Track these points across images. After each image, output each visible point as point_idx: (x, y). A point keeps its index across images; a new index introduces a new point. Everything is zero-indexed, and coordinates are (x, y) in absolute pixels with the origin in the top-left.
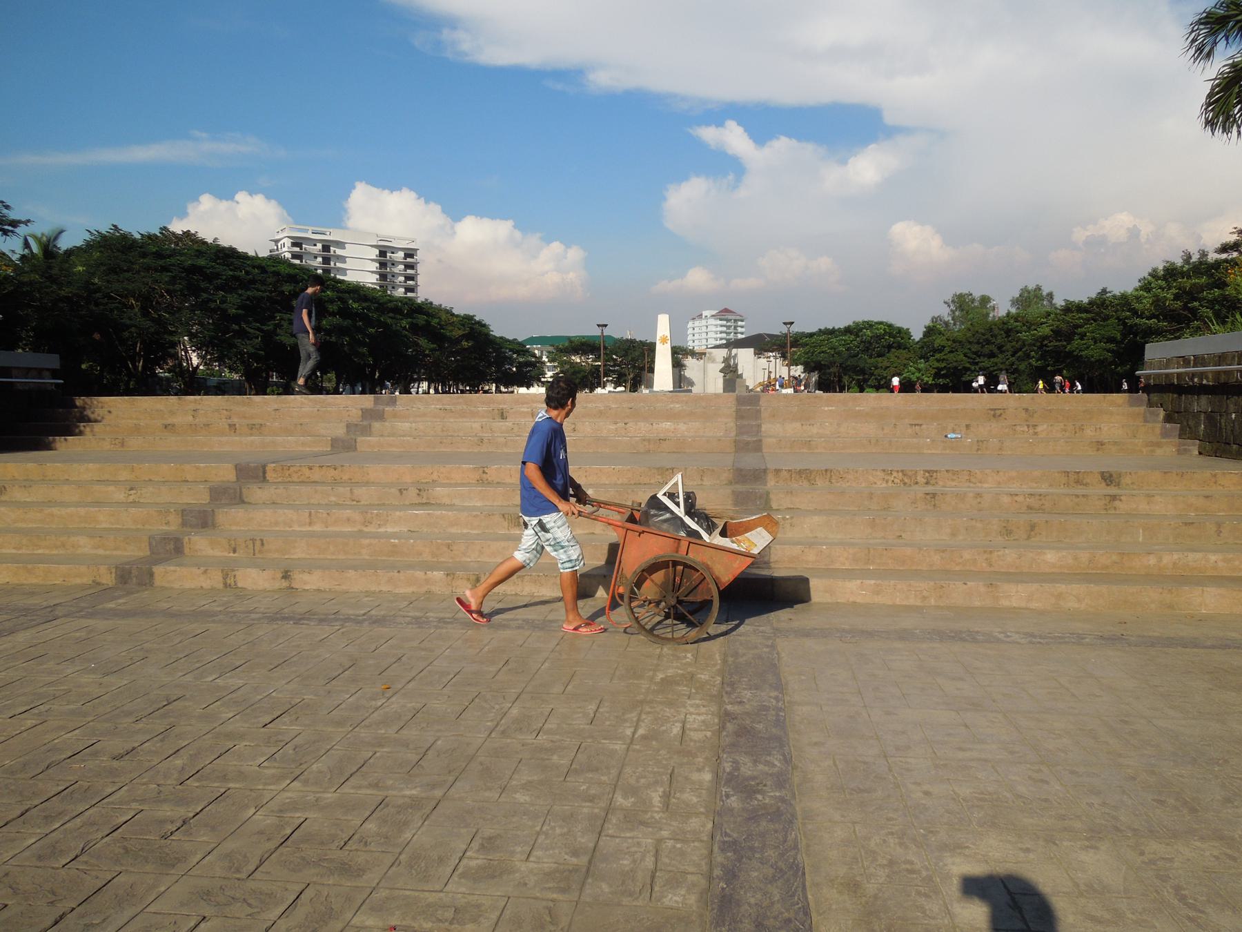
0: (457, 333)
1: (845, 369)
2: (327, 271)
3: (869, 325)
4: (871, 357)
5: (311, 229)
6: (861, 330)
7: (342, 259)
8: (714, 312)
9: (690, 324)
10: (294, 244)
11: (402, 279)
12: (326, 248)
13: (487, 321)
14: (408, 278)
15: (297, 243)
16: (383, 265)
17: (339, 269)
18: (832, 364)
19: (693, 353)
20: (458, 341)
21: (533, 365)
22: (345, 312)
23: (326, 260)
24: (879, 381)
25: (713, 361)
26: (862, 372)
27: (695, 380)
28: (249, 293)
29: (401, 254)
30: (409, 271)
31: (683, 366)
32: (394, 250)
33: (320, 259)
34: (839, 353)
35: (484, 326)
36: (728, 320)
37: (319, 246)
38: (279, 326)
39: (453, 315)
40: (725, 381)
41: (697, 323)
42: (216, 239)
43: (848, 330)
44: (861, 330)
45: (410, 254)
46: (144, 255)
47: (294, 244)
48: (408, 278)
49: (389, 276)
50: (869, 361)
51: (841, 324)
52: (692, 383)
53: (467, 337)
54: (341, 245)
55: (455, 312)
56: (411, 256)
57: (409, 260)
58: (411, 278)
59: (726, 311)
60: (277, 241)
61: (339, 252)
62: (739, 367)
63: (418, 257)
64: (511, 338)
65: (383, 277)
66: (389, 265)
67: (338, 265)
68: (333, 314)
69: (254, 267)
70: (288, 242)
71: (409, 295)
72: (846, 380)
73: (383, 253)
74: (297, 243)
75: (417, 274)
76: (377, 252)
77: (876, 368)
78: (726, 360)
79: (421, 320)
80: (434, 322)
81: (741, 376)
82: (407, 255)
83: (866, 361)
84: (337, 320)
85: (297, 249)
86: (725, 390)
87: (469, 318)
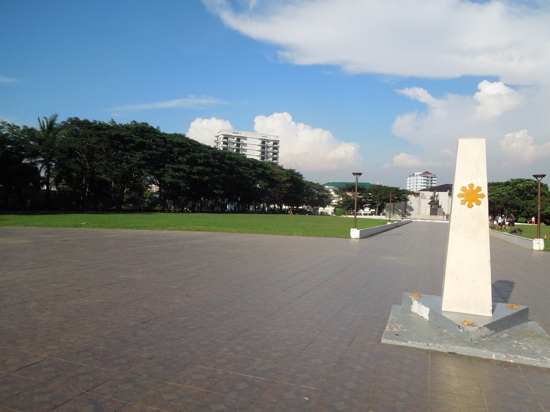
0: (284, 179)
1: (506, 205)
2: (238, 150)
3: (522, 181)
4: (523, 199)
6: (516, 183)
7: (245, 145)
8: (421, 173)
9: (408, 179)
10: (224, 138)
11: (271, 154)
12: (238, 140)
13: (301, 173)
14: (274, 154)
15: (226, 137)
16: (263, 148)
17: (244, 150)
18: (499, 203)
20: (284, 183)
21: (327, 197)
22: (207, 164)
23: (238, 145)
24: (528, 214)
25: (425, 198)
26: (518, 208)
27: (414, 208)
28: (150, 152)
29: (272, 143)
30: (275, 151)
31: (408, 200)
32: (269, 141)
33: (235, 145)
34: (502, 196)
35: (301, 176)
36: (427, 177)
37: (236, 139)
38: (165, 171)
39: (283, 170)
40: (431, 209)
41: (412, 178)
42: (158, 127)
43: (507, 184)
44: (516, 183)
45: (276, 143)
46: (90, 128)
47: (224, 138)
48: (274, 154)
49: (266, 153)
50: (522, 202)
51: (503, 180)
52: (412, 209)
53: (288, 181)
54: (245, 138)
55: (285, 167)
56: (276, 144)
58: (276, 154)
59: (427, 172)
60: (217, 137)
61: (244, 141)
63: (280, 144)
64: (316, 183)
65: (263, 153)
66: (266, 147)
67: (243, 147)
68: (201, 165)
69: (160, 138)
70: (222, 137)
71: (274, 161)
72: (506, 211)
73: (263, 142)
74: (226, 137)
75: (278, 152)
76: (261, 141)
77: (527, 206)
78: (432, 198)
79: (260, 170)
80: (268, 172)
81: (440, 207)
82: (274, 143)
83: (519, 201)
84: (201, 168)
85: (226, 140)
87: (291, 172)
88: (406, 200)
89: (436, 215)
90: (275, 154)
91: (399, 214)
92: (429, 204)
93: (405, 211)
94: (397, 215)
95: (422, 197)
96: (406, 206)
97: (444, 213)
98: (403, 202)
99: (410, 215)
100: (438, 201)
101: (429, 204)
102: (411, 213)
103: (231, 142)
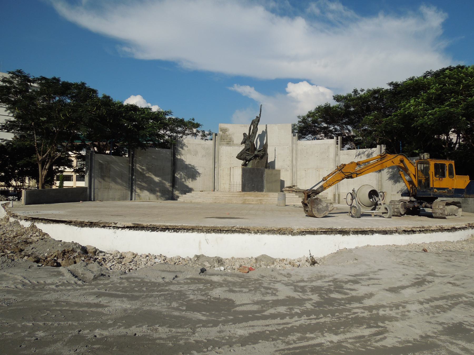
19: (190, 126)
25: (229, 142)
27: (200, 171)
40: (243, 170)
62: (270, 151)
78: (248, 139)
86: (244, 189)
88: (173, 146)
89: (260, 189)
91: (152, 191)
92: (239, 157)
93: (174, 181)
94: (146, 194)
95: (222, 139)
96: (176, 164)
97: (282, 182)
98: (167, 152)
99: (188, 190)
100: (264, 148)
101: (239, 157)
102: (190, 183)
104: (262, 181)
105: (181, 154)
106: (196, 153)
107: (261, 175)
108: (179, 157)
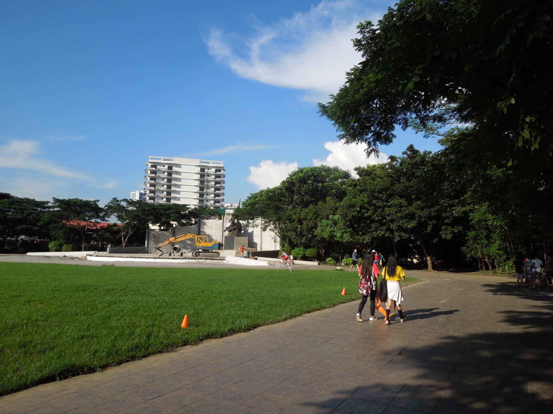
5: (162, 158)
12: (170, 168)
16: (202, 176)
23: (170, 174)
29: (214, 170)
33: (166, 174)
37: (166, 167)
47: (152, 166)
48: (217, 183)
56: (220, 171)
57: (218, 173)
65: (202, 182)
70: (150, 165)
73: (203, 170)
82: (216, 171)
85: (154, 169)
90: (217, 183)
103: (159, 170)
104: (233, 244)
105: (203, 228)
106: (212, 228)
107: (234, 239)
108: (202, 230)
